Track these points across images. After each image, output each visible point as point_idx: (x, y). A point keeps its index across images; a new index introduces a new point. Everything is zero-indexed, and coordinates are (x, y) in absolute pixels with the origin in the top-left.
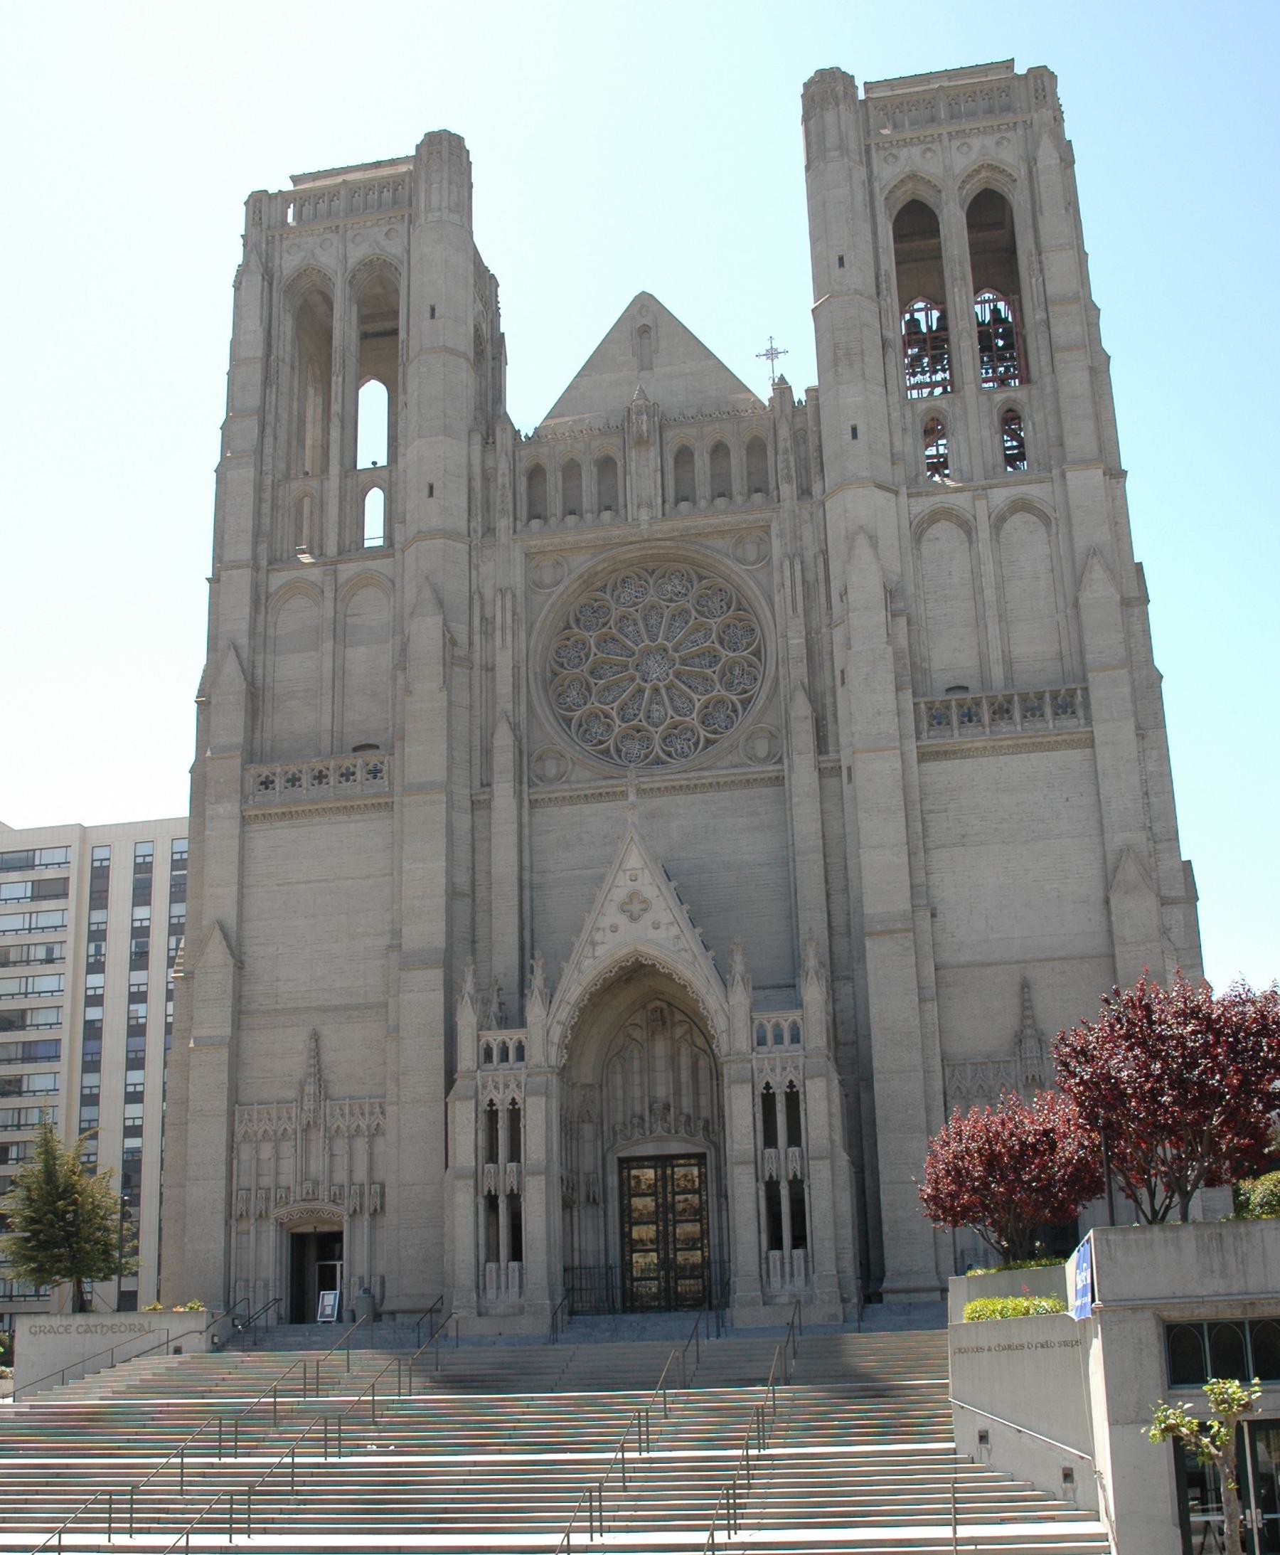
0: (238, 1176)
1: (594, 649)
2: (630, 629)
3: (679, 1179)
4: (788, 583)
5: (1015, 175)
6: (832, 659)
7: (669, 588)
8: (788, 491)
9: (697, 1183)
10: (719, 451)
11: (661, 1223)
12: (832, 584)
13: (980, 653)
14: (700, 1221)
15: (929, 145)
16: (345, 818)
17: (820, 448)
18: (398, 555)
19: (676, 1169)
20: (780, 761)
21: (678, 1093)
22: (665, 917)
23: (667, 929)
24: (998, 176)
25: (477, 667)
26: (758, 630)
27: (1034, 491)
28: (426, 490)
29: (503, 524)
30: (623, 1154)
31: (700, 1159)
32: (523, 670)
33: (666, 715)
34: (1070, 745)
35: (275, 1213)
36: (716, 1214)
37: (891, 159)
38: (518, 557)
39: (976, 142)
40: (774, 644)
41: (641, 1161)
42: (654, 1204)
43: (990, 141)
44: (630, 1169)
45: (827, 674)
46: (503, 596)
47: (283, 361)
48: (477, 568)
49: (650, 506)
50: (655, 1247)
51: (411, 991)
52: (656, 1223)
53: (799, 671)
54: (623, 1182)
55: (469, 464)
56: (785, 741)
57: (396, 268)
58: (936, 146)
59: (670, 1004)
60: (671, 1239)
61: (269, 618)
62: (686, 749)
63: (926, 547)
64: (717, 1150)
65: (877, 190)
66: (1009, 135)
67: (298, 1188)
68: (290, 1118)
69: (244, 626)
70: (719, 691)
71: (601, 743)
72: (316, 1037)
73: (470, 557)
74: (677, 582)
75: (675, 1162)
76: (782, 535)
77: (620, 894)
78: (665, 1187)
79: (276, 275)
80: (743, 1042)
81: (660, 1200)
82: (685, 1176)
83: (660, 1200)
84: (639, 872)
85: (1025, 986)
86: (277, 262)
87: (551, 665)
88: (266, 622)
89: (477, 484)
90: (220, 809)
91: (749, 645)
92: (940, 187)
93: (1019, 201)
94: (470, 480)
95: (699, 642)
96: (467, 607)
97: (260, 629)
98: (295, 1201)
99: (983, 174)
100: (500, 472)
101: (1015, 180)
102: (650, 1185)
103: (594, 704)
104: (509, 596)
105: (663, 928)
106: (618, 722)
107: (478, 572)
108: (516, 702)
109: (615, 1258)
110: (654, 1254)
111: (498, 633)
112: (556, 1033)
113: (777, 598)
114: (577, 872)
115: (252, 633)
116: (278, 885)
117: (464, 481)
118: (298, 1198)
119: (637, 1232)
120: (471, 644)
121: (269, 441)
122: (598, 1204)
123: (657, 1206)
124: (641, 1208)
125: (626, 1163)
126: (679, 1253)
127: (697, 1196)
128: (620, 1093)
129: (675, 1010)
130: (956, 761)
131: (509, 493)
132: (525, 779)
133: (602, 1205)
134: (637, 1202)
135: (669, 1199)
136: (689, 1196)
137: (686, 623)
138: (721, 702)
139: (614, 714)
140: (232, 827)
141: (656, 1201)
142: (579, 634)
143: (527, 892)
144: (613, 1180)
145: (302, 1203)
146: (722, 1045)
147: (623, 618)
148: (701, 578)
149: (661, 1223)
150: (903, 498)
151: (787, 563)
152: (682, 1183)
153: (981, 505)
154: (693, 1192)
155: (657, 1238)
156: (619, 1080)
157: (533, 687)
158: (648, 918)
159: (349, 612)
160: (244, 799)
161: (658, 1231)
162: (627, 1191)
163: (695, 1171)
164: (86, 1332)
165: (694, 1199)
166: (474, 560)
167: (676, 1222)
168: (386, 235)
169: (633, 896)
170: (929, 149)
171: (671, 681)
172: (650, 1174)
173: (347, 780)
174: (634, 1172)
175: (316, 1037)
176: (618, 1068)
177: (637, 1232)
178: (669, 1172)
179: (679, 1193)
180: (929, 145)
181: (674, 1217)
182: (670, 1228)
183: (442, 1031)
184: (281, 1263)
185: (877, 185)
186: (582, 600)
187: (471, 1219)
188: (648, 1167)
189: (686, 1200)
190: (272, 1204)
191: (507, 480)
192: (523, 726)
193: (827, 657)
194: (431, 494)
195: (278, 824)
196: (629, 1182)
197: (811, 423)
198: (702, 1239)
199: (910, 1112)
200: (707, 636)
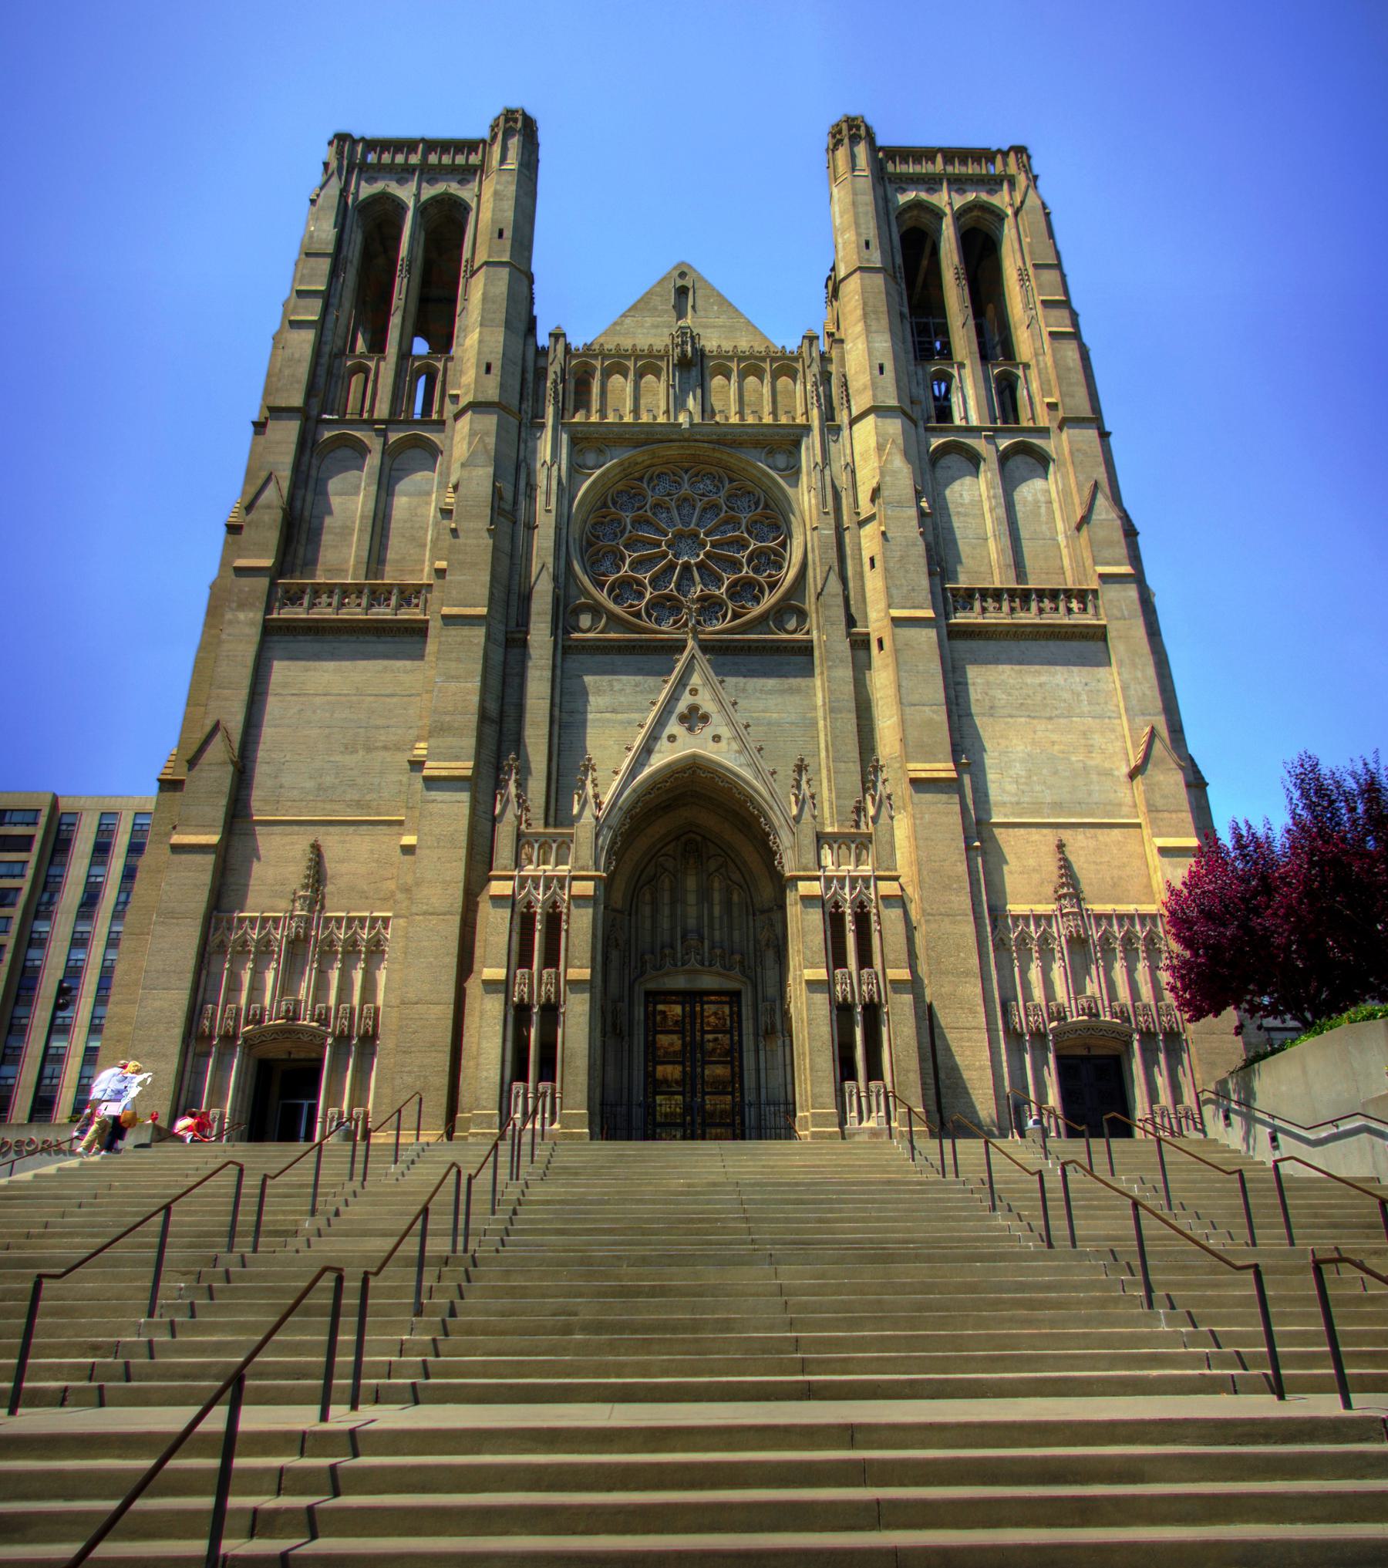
0: (205, 990)
1: (629, 527)
2: (664, 515)
3: (708, 1017)
7: (702, 486)
9: (728, 1022)
11: (688, 1064)
12: (859, 489)
14: (731, 1063)
16: (374, 639)
17: (845, 385)
18: (450, 422)
19: (706, 1006)
20: (808, 633)
21: (711, 928)
22: (725, 732)
23: (729, 744)
24: (987, 216)
28: (484, 368)
30: (651, 986)
31: (734, 996)
36: (752, 1054)
40: (802, 538)
41: (667, 996)
42: (680, 1042)
44: (655, 1004)
47: (351, 262)
48: (526, 442)
50: (681, 1089)
52: (683, 1063)
54: (650, 1016)
55: (524, 359)
56: (814, 615)
59: (704, 837)
60: (699, 1081)
61: (314, 461)
64: (755, 987)
65: (891, 212)
72: (316, 848)
73: (520, 432)
75: (705, 999)
77: (682, 706)
78: (693, 1024)
81: (688, 1039)
82: (715, 1014)
83: (688, 1039)
84: (700, 689)
85: (1061, 846)
87: (588, 537)
88: (310, 463)
89: (530, 377)
96: (513, 472)
97: (304, 468)
99: (975, 213)
102: (677, 1021)
105: (723, 744)
107: (526, 447)
109: (639, 1096)
110: (679, 1098)
112: (606, 839)
114: (608, 715)
116: (293, 695)
117: (519, 369)
119: (663, 1071)
121: (331, 318)
122: (623, 1038)
123: (684, 1045)
124: (666, 1045)
125: (654, 997)
126: (707, 1097)
127: (728, 1036)
128: (648, 924)
129: (709, 844)
130: (981, 642)
132: (560, 625)
133: (626, 1038)
134: (663, 1040)
135: (698, 1038)
136: (720, 1036)
137: (718, 514)
140: (254, 633)
141: (683, 1039)
142: (614, 513)
143: (556, 727)
144: (639, 1012)
147: (657, 506)
148: (731, 481)
149: (688, 1064)
150: (921, 430)
152: (712, 1019)
154: (724, 1032)
155: (683, 1080)
156: (647, 910)
157: (572, 549)
158: (709, 731)
159: (395, 466)
160: (269, 609)
161: (684, 1072)
162: (654, 1025)
163: (727, 1009)
165: (724, 1039)
166: (523, 435)
167: (704, 1063)
169: (693, 709)
171: (702, 560)
172: (678, 1009)
174: (660, 1007)
175: (316, 848)
176: (648, 897)
177: (663, 1071)
178: (698, 1009)
179: (709, 1032)
181: (703, 1057)
182: (699, 1070)
183: (464, 844)
184: (243, 1092)
186: (620, 486)
187: (499, 1028)
188: (675, 1003)
189: (716, 1040)
195: (301, 638)
196: (654, 1016)
198: (733, 1082)
199: (962, 955)
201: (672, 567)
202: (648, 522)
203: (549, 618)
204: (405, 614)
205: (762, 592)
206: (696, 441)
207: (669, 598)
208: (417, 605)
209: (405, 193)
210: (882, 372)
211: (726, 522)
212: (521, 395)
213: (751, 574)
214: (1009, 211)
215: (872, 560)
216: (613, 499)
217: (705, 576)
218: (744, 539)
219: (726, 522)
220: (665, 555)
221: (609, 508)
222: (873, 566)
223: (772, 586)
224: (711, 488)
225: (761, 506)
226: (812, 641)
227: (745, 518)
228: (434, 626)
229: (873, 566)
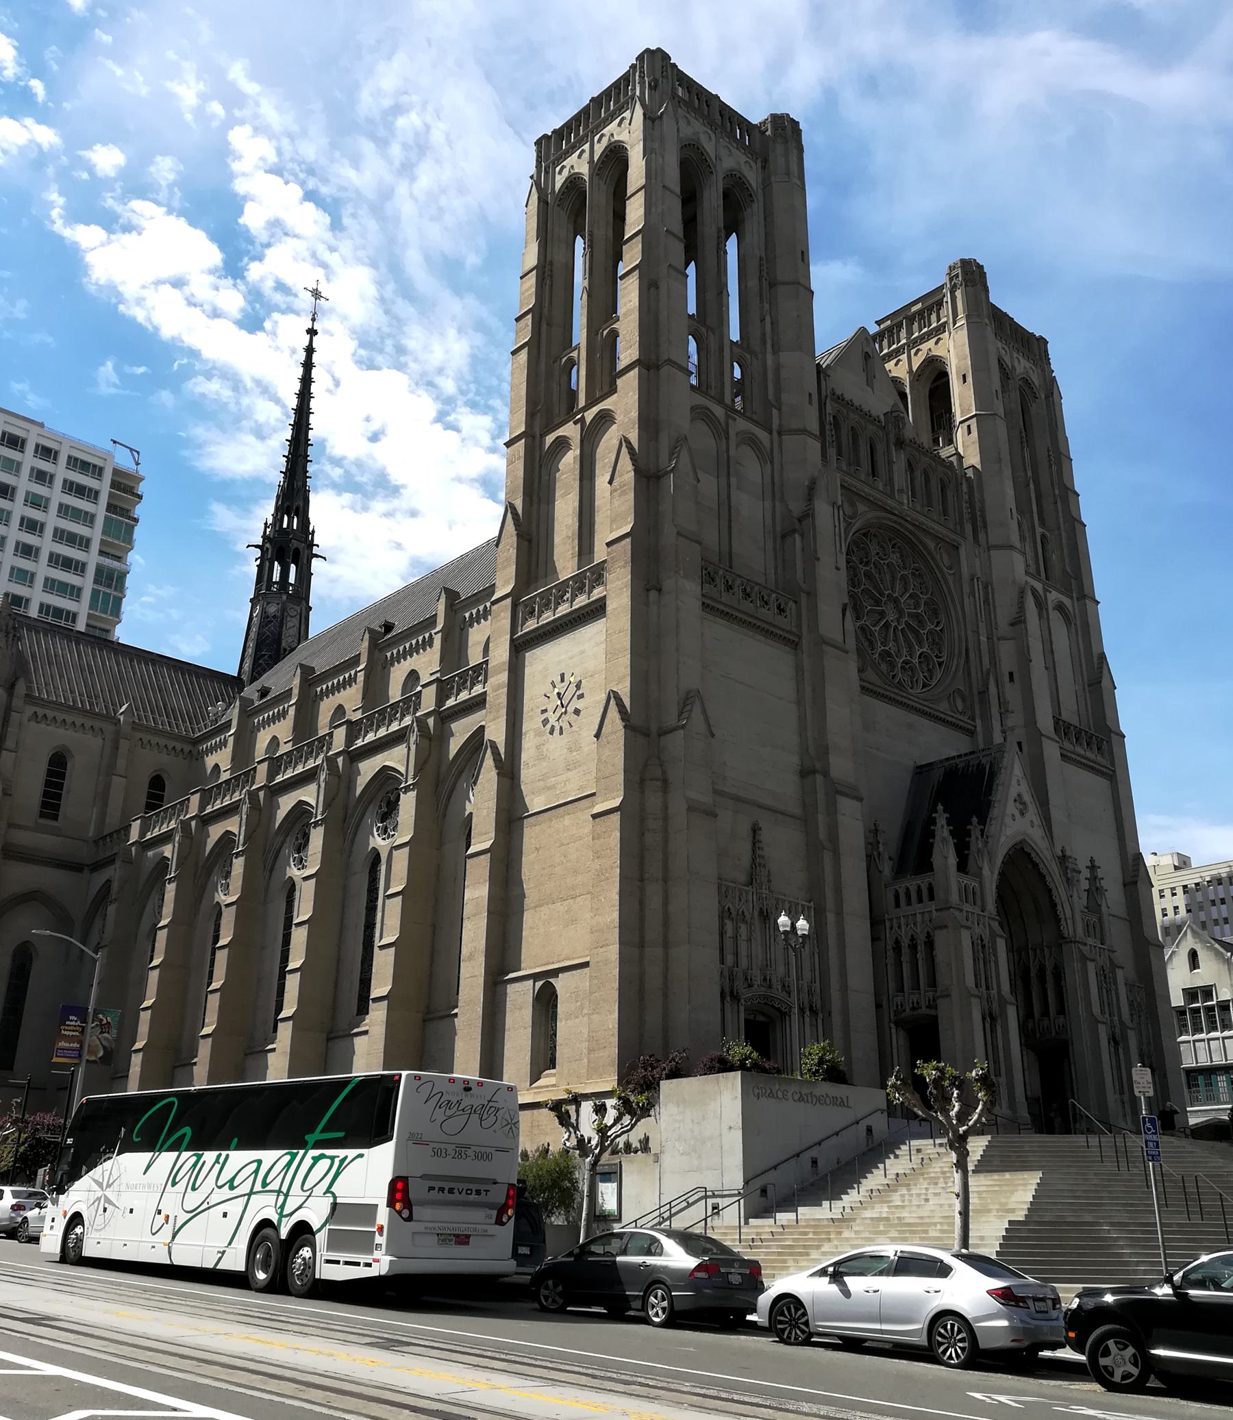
8: (968, 528)
17: (982, 510)
18: (775, 433)
22: (1037, 822)
26: (942, 617)
27: (1067, 601)
34: (1102, 774)
51: (844, 814)
53: (986, 660)
56: (977, 707)
72: (755, 830)
77: (1013, 793)
80: (1080, 930)
91: (938, 623)
113: (966, 601)
116: (722, 676)
146: (1068, 929)
151: (975, 580)
175: (755, 830)
200: (917, 606)
201: (887, 625)
206: (906, 520)
215: (1011, 674)
223: (940, 664)
226: (975, 727)
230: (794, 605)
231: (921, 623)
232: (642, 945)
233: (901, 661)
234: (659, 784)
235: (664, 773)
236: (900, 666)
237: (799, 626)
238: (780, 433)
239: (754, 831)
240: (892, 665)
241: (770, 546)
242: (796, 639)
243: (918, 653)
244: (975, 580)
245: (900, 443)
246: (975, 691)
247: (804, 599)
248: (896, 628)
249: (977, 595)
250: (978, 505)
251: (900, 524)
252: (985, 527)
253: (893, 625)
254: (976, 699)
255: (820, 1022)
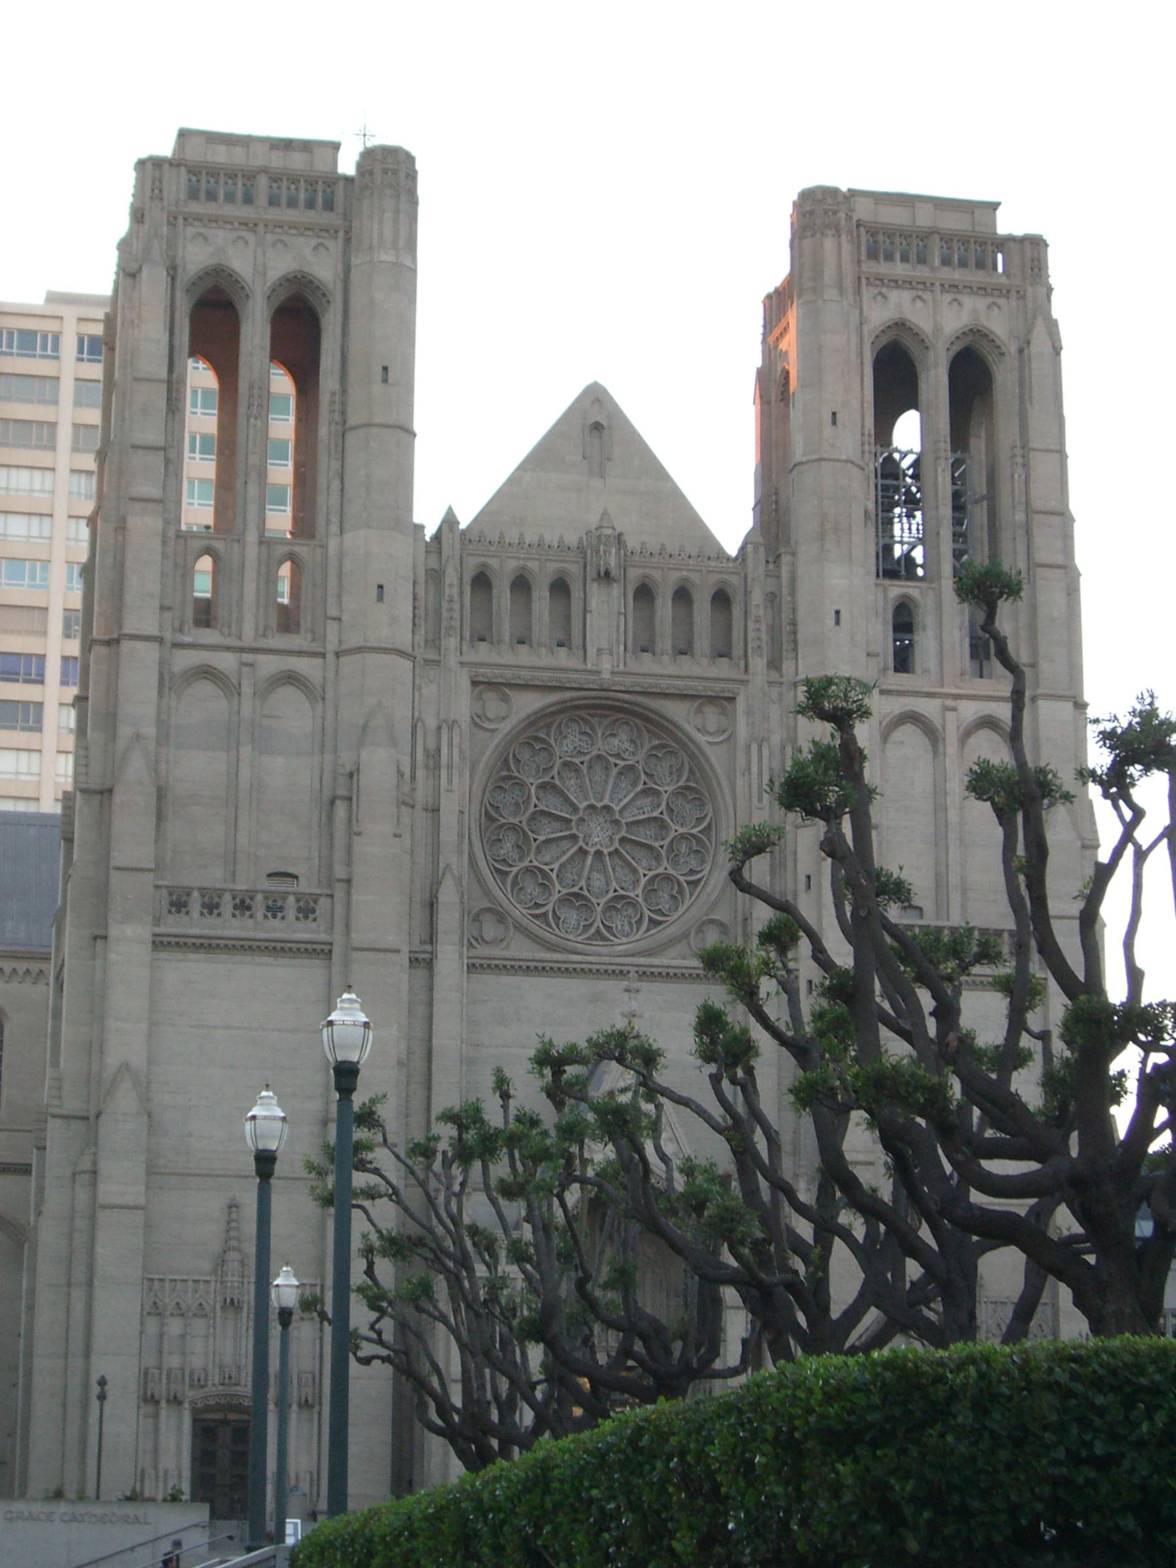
2: (572, 782)
4: (755, 769)
5: (1004, 349)
6: (795, 860)
8: (758, 664)
10: (683, 595)
13: (937, 874)
15: (920, 293)
16: (270, 960)
17: (794, 624)
18: (330, 657)
25: (418, 807)
26: (709, 808)
28: (374, 592)
29: (452, 642)
32: (466, 816)
33: (607, 885)
35: (190, 1394)
37: (879, 298)
38: (465, 683)
39: (968, 301)
43: (981, 303)
45: (789, 876)
46: (451, 728)
48: (420, 688)
49: (611, 653)
55: (414, 567)
57: (324, 295)
58: (927, 296)
62: (627, 928)
63: (891, 750)
65: (865, 332)
66: (1001, 301)
67: (217, 1370)
68: (208, 1292)
69: (151, 712)
70: (664, 867)
71: (538, 906)
74: (624, 737)
76: (749, 712)
79: (180, 270)
86: (180, 252)
90: (129, 931)
91: (700, 820)
92: (928, 344)
93: (1004, 377)
94: (415, 583)
95: (645, 809)
98: (213, 1385)
100: (448, 581)
101: (1003, 354)
103: (532, 859)
104: (456, 731)
106: (558, 887)
107: (420, 695)
108: (460, 853)
111: (444, 773)
113: (740, 781)
115: (160, 722)
118: (217, 1381)
120: (413, 778)
131: (457, 606)
138: (667, 878)
139: (554, 875)
142: (516, 778)
145: (221, 1388)
151: (754, 748)
153: (950, 715)
160: (157, 921)
164: (71, 1521)
166: (417, 681)
168: (315, 249)
170: (919, 297)
171: (616, 850)
173: (274, 917)
180: (920, 293)
185: (866, 328)
190: (187, 1386)
191: (455, 591)
192: (465, 882)
193: (790, 858)
194: (380, 598)
195: (191, 956)
197: (785, 591)
201: (582, 852)
202: (554, 786)
203: (456, 937)
204: (304, 932)
205: (681, 891)
207: (577, 896)
208: (315, 920)
209: (241, 263)
210: (838, 622)
211: (647, 792)
212: (414, 625)
213: (671, 871)
214: (1013, 349)
215: (809, 877)
216: (514, 755)
217: (618, 869)
218: (663, 820)
219: (647, 792)
220: (574, 838)
221: (509, 770)
222: (809, 887)
223: (694, 884)
224: (627, 745)
225: (699, 829)
227: (667, 788)
228: (337, 951)
229: (809, 887)
230: (328, 900)
231: (662, 825)
232: (66, 1355)
233: (603, 901)
234: (86, 1177)
235: (95, 1163)
236: (599, 909)
237: (331, 928)
238: (337, 655)
239: (230, 1207)
240: (588, 907)
241: (315, 820)
242: (327, 948)
243: (643, 881)
244: (754, 748)
245: (606, 577)
246: (740, 919)
247: (339, 891)
248: (599, 853)
249: (755, 769)
250: (785, 616)
251: (607, 699)
252: (795, 649)
253: (592, 850)
254: (740, 930)
255: (316, 1416)
